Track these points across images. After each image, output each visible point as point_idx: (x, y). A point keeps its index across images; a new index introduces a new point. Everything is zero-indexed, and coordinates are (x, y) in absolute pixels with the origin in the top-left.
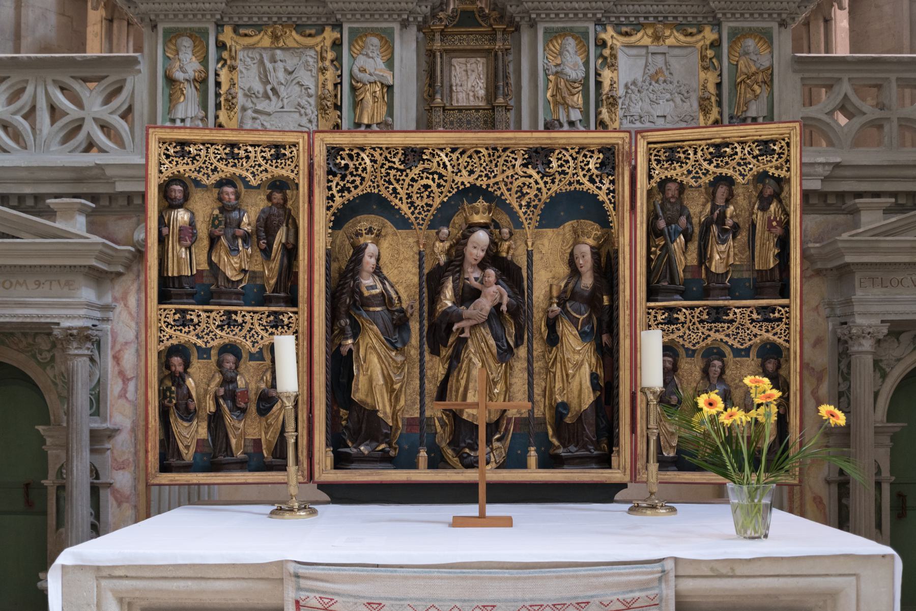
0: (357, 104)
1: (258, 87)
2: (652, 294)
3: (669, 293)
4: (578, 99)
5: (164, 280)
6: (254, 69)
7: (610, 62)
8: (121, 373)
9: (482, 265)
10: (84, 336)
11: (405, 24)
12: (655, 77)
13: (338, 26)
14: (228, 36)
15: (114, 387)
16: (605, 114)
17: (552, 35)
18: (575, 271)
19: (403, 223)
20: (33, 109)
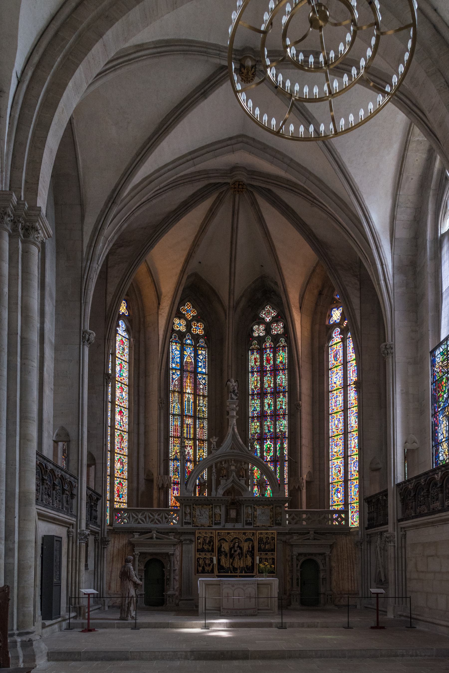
0: (215, 517)
1: (199, 514)
2: (259, 551)
3: (261, 551)
4: (251, 517)
5: (197, 549)
6: (199, 511)
7: (256, 511)
8: (177, 560)
9: (237, 547)
10: (173, 555)
11: (223, 504)
12: (263, 513)
13: (212, 504)
14: (195, 506)
15: (176, 563)
16: (255, 519)
17: (247, 506)
18: (249, 548)
19: (227, 541)
20: (162, 516)
